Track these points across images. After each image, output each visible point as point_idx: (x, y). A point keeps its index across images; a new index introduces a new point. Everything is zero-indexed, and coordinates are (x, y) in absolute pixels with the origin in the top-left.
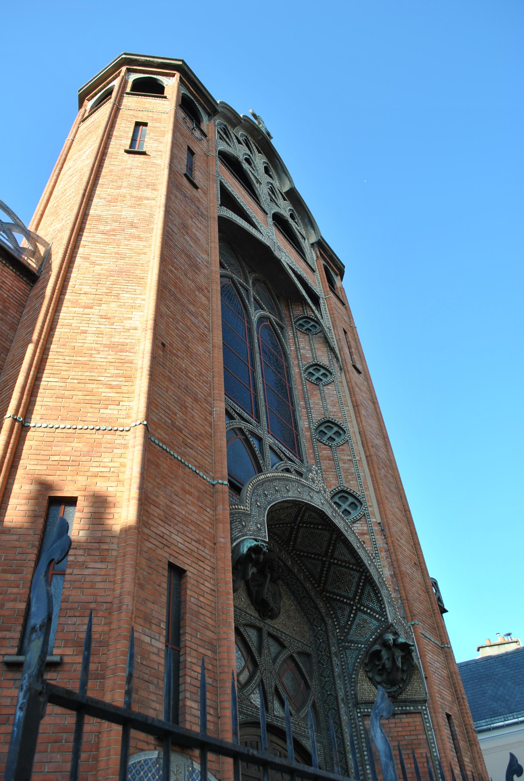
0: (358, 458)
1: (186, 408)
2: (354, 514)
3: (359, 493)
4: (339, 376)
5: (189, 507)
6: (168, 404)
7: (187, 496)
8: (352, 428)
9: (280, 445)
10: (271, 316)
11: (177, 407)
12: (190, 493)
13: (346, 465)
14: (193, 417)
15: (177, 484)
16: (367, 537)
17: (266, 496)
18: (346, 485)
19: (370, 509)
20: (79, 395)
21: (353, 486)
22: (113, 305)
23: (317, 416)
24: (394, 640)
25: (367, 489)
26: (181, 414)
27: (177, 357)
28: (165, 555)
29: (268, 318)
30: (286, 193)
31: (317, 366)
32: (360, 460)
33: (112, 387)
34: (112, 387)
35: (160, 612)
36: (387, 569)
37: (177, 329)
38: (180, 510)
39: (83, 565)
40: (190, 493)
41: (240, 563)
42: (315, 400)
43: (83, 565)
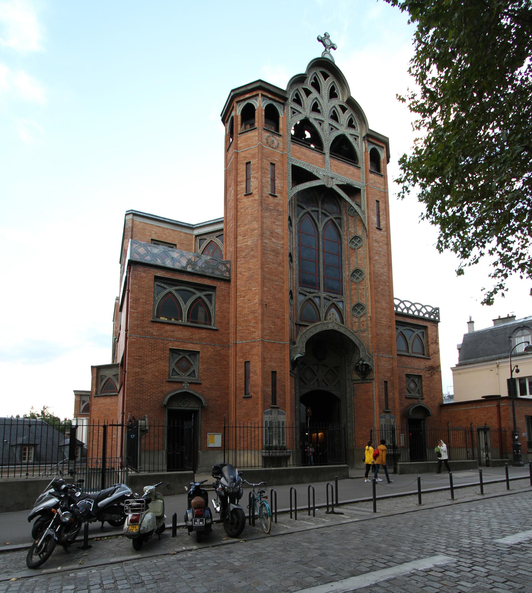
2: (362, 313)
4: (365, 241)
8: (366, 271)
9: (330, 294)
18: (360, 301)
20: (246, 331)
21: (363, 301)
22: (250, 294)
23: (352, 269)
25: (368, 301)
27: (271, 306)
28: (270, 370)
31: (356, 237)
33: (253, 327)
34: (253, 327)
35: (270, 383)
37: (271, 294)
39: (253, 377)
41: (294, 364)
42: (353, 259)
43: (253, 377)
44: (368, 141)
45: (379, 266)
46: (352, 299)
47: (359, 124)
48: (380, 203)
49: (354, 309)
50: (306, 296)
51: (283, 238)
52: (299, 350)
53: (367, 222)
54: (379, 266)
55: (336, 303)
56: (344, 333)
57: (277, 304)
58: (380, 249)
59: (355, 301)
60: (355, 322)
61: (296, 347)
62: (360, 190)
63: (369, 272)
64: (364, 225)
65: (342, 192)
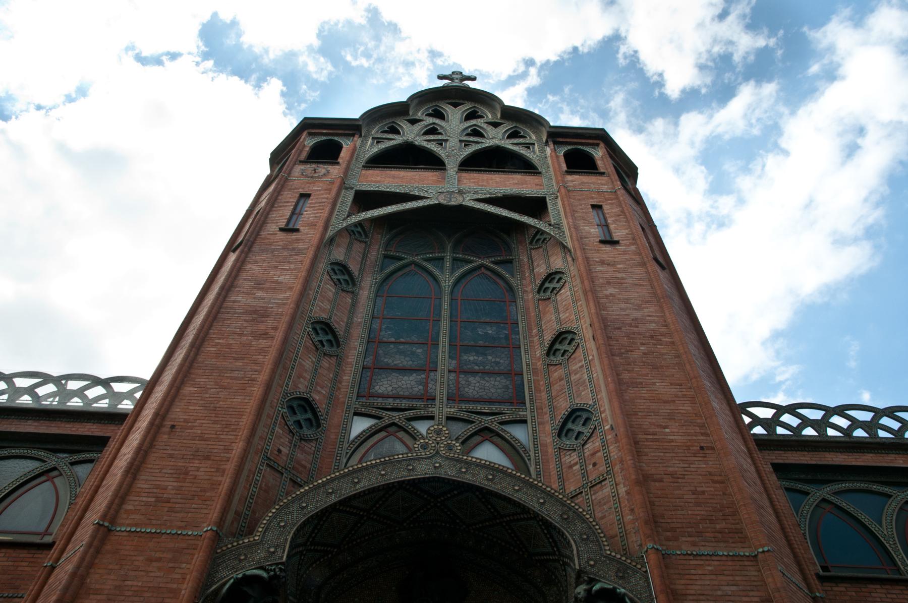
0: (591, 358)
1: (186, 473)
3: (591, 402)
5: (152, 574)
6: (158, 483)
7: (154, 564)
10: (486, 262)
11: (171, 479)
12: (159, 560)
13: (578, 376)
14: (195, 477)
15: (141, 558)
16: (599, 454)
17: (303, 508)
19: (603, 415)
21: (585, 398)
24: (589, 591)
26: (175, 484)
27: (191, 428)
29: (482, 266)
30: (503, 117)
32: (593, 359)
36: (622, 486)
37: (203, 399)
38: (135, 583)
40: (159, 560)
44: (555, 143)
45: (623, 306)
46: (553, 409)
47: (534, 133)
48: (606, 207)
49: (562, 431)
50: (379, 418)
51: (291, 288)
52: (261, 554)
53: (568, 239)
54: (623, 306)
55: (495, 426)
56: (486, 484)
57: (215, 422)
58: (620, 275)
59: (564, 406)
60: (571, 467)
61: (250, 546)
62: (545, 198)
63: (588, 322)
64: (564, 247)
65: (491, 206)
